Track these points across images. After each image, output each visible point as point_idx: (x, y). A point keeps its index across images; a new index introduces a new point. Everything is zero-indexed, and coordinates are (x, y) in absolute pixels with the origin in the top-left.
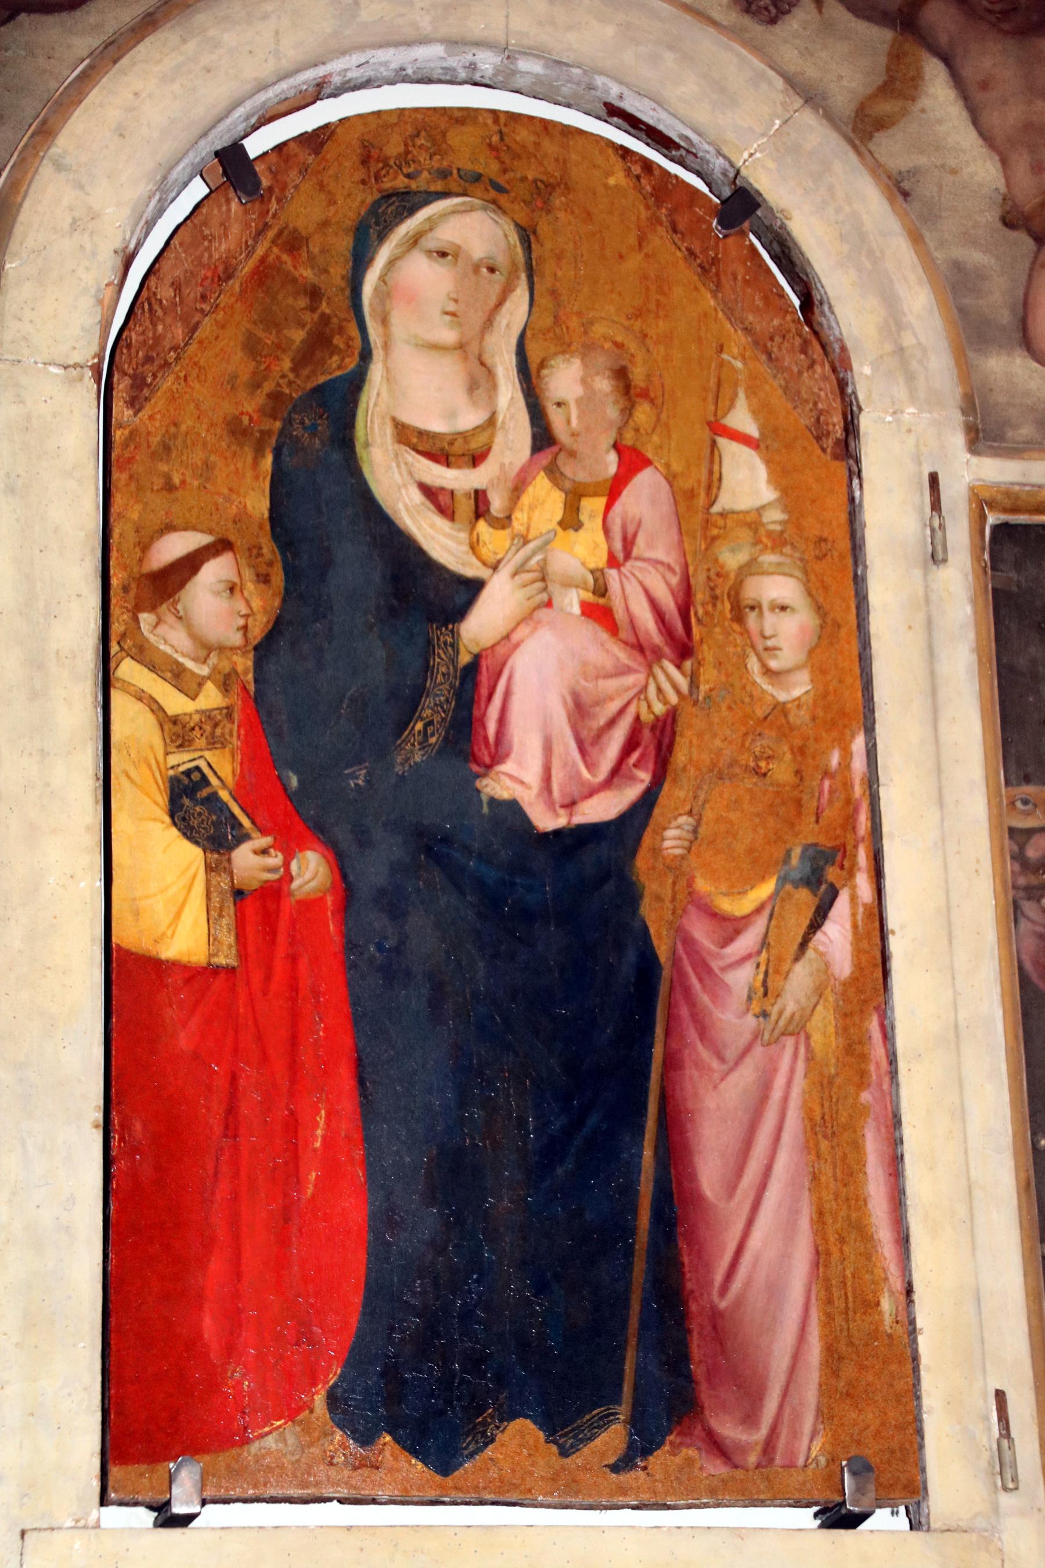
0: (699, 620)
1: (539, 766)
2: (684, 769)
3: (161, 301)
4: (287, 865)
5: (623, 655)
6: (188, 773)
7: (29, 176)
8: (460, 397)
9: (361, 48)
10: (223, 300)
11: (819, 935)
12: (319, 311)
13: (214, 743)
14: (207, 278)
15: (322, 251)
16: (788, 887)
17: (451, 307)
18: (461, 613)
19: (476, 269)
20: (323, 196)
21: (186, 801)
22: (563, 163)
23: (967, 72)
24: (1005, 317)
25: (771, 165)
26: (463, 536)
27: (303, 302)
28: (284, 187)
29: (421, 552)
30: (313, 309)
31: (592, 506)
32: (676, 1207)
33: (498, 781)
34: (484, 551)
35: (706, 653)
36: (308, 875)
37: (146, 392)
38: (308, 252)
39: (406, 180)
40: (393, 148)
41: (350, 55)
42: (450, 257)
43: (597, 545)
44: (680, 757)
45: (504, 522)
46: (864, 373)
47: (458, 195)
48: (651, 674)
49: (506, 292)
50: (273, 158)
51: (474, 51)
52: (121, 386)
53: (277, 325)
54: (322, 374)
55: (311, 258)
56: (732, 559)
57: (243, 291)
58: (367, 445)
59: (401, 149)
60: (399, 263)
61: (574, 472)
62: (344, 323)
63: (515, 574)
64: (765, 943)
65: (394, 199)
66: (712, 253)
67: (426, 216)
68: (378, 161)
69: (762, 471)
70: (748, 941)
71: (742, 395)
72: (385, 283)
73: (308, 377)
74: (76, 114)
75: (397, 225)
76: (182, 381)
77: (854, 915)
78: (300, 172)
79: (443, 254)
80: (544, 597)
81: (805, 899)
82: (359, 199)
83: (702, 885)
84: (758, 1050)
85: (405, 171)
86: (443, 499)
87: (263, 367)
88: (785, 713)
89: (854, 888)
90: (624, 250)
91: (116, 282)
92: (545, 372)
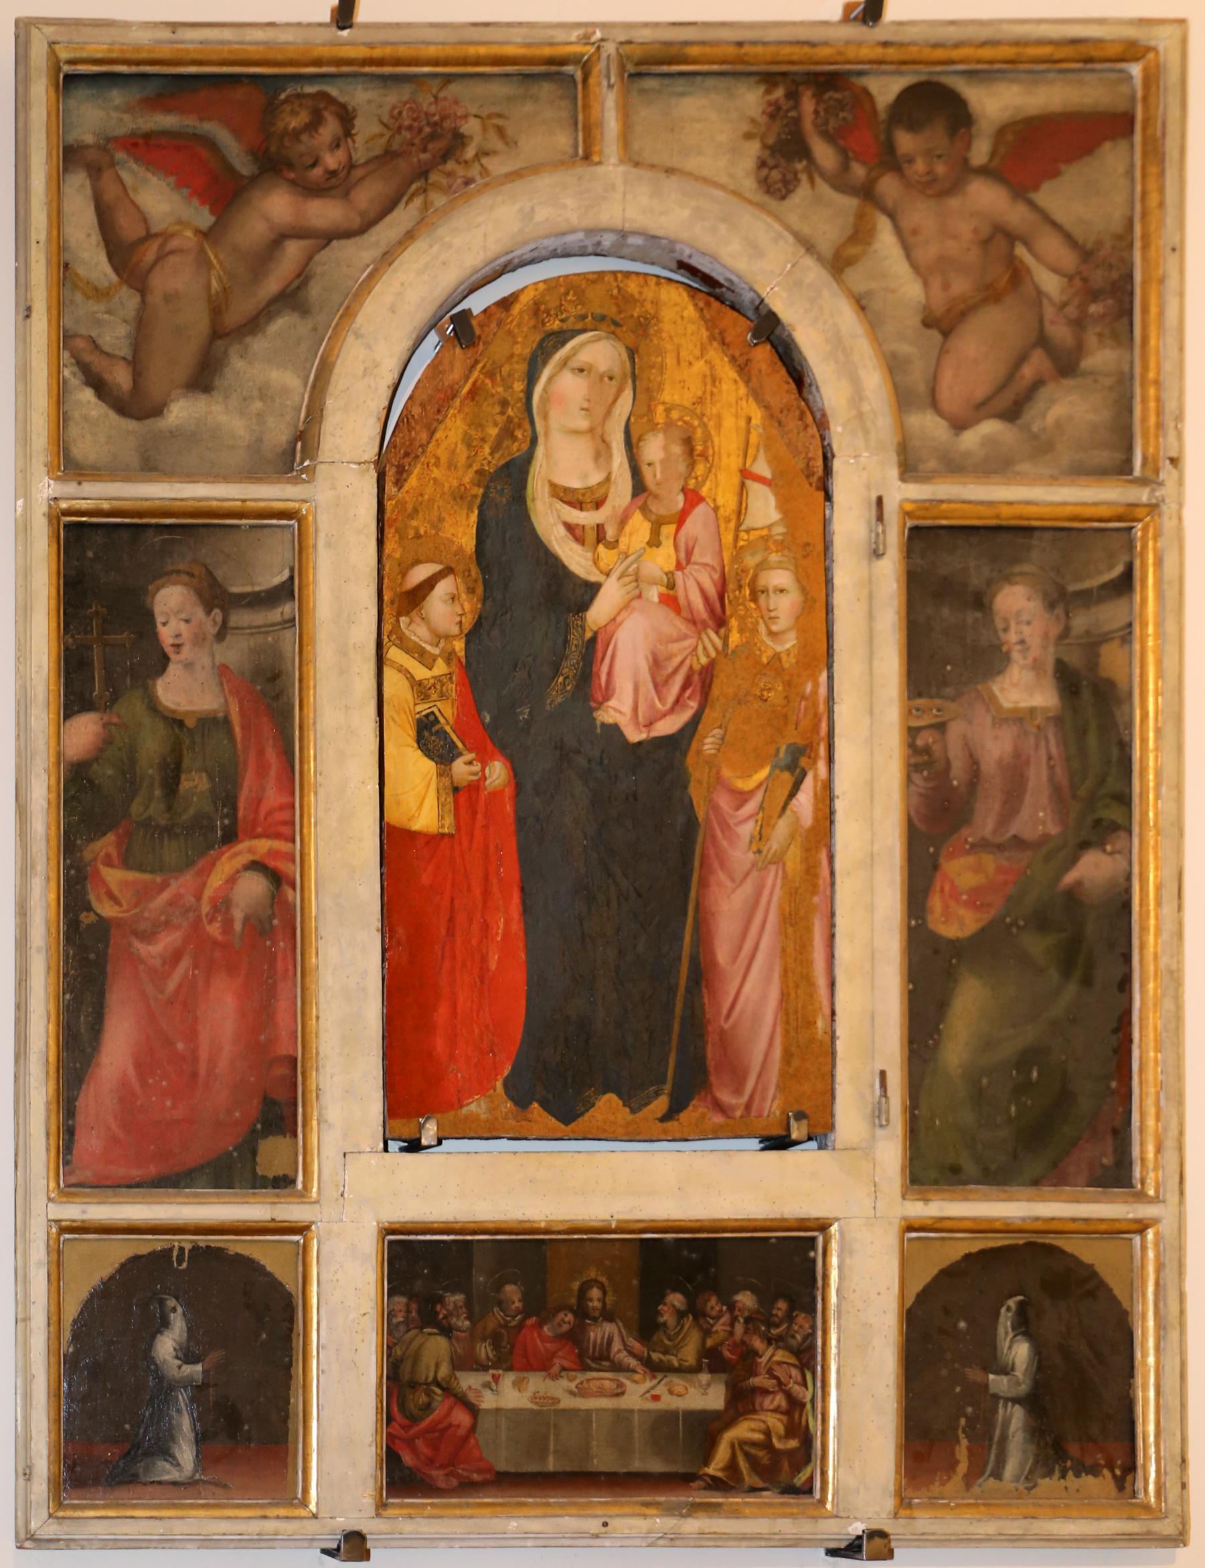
0: (730, 602)
1: (630, 704)
2: (718, 699)
4: (483, 770)
5: (683, 627)
6: (427, 716)
8: (589, 464)
10: (452, 411)
11: (794, 801)
13: (443, 696)
15: (509, 375)
16: (777, 771)
17: (585, 405)
18: (585, 606)
19: (601, 377)
21: (426, 734)
22: (656, 303)
23: (905, 224)
24: (922, 388)
25: (784, 295)
26: (589, 555)
27: (498, 409)
29: (564, 567)
30: (502, 413)
31: (668, 530)
32: (702, 974)
33: (607, 712)
34: (602, 564)
35: (734, 623)
36: (495, 777)
37: (405, 475)
43: (670, 556)
44: (716, 691)
45: (613, 545)
46: (838, 433)
48: (700, 638)
49: (620, 391)
56: (751, 561)
58: (533, 500)
59: (558, 303)
61: (657, 508)
63: (619, 578)
64: (761, 807)
66: (746, 357)
69: (772, 501)
70: (751, 807)
71: (762, 451)
77: (815, 787)
79: (581, 370)
80: (637, 591)
81: (787, 778)
83: (726, 773)
84: (754, 874)
86: (578, 532)
88: (780, 660)
89: (816, 770)
90: (691, 358)
92: (641, 444)
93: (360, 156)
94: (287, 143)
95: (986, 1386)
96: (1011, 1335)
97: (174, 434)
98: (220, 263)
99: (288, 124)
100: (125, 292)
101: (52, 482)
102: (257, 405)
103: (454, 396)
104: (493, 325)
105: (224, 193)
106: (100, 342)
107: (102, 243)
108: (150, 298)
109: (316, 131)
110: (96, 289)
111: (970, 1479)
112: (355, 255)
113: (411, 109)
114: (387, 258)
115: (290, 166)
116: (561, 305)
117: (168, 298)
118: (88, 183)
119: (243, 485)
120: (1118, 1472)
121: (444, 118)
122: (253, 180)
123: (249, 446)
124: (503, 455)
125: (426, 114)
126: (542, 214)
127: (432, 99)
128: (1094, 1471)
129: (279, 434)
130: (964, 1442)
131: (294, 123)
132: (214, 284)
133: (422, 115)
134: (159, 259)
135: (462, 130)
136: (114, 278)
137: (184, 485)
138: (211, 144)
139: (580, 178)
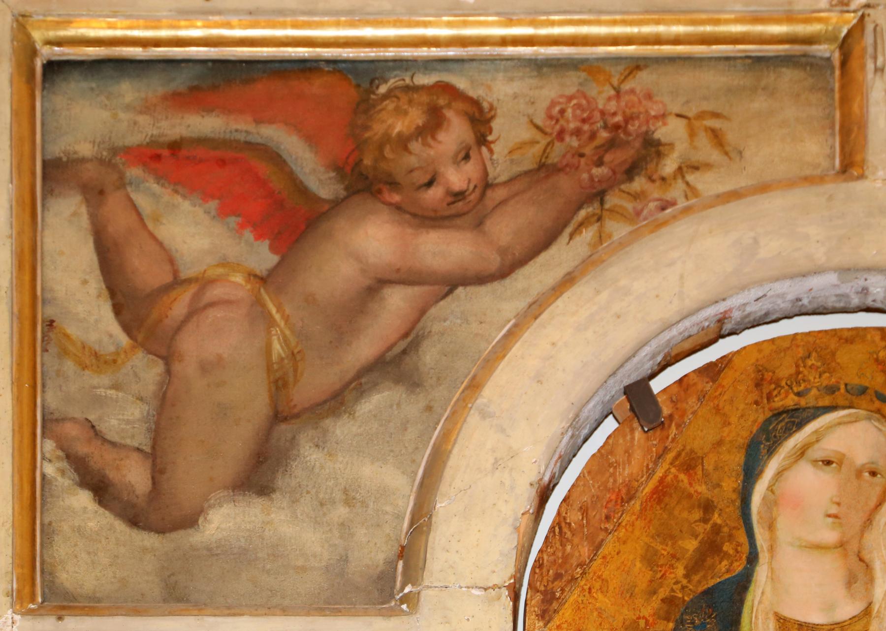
3: (570, 524)
7: (459, 426)
8: (838, 591)
9: (760, 283)
10: (626, 518)
12: (711, 522)
14: (611, 500)
15: (716, 469)
17: (834, 510)
19: (859, 473)
20: (718, 419)
27: (697, 515)
28: (683, 414)
30: (705, 521)
37: (555, 605)
38: (703, 470)
39: (796, 398)
40: (785, 371)
41: (749, 290)
42: (834, 465)
47: (844, 408)
50: (676, 389)
51: (865, 276)
52: (533, 602)
53: (672, 537)
54: (712, 578)
55: (706, 475)
57: (643, 509)
59: (793, 370)
60: (786, 473)
62: (734, 531)
65: (784, 415)
67: (813, 430)
68: (770, 383)
72: (772, 491)
73: (699, 582)
74: (500, 367)
75: (786, 439)
76: (587, 593)
78: (699, 399)
79: (828, 463)
82: (751, 419)
85: (795, 389)
87: (659, 575)
91: (531, 511)
93: (500, 171)
94: (388, 152)
97: (211, 552)
98: (287, 319)
99: (392, 127)
100: (140, 359)
101: (17, 617)
102: (341, 512)
103: (631, 498)
104: (692, 401)
105: (291, 222)
106: (102, 427)
107: (105, 293)
108: (177, 367)
109: (434, 138)
110: (96, 355)
112: (490, 307)
113: (578, 106)
114: (536, 309)
115: (394, 185)
116: (798, 373)
117: (205, 368)
118: (84, 210)
119: (310, 619)
121: (628, 119)
122: (336, 204)
123: (327, 567)
124: (705, 577)
125: (603, 113)
126: (772, 247)
127: (612, 92)
129: (373, 550)
131: (400, 126)
132: (277, 348)
133: (597, 115)
134: (193, 312)
135: (657, 135)
136: (123, 339)
137: (220, 619)
138: (275, 158)
139: (830, 198)
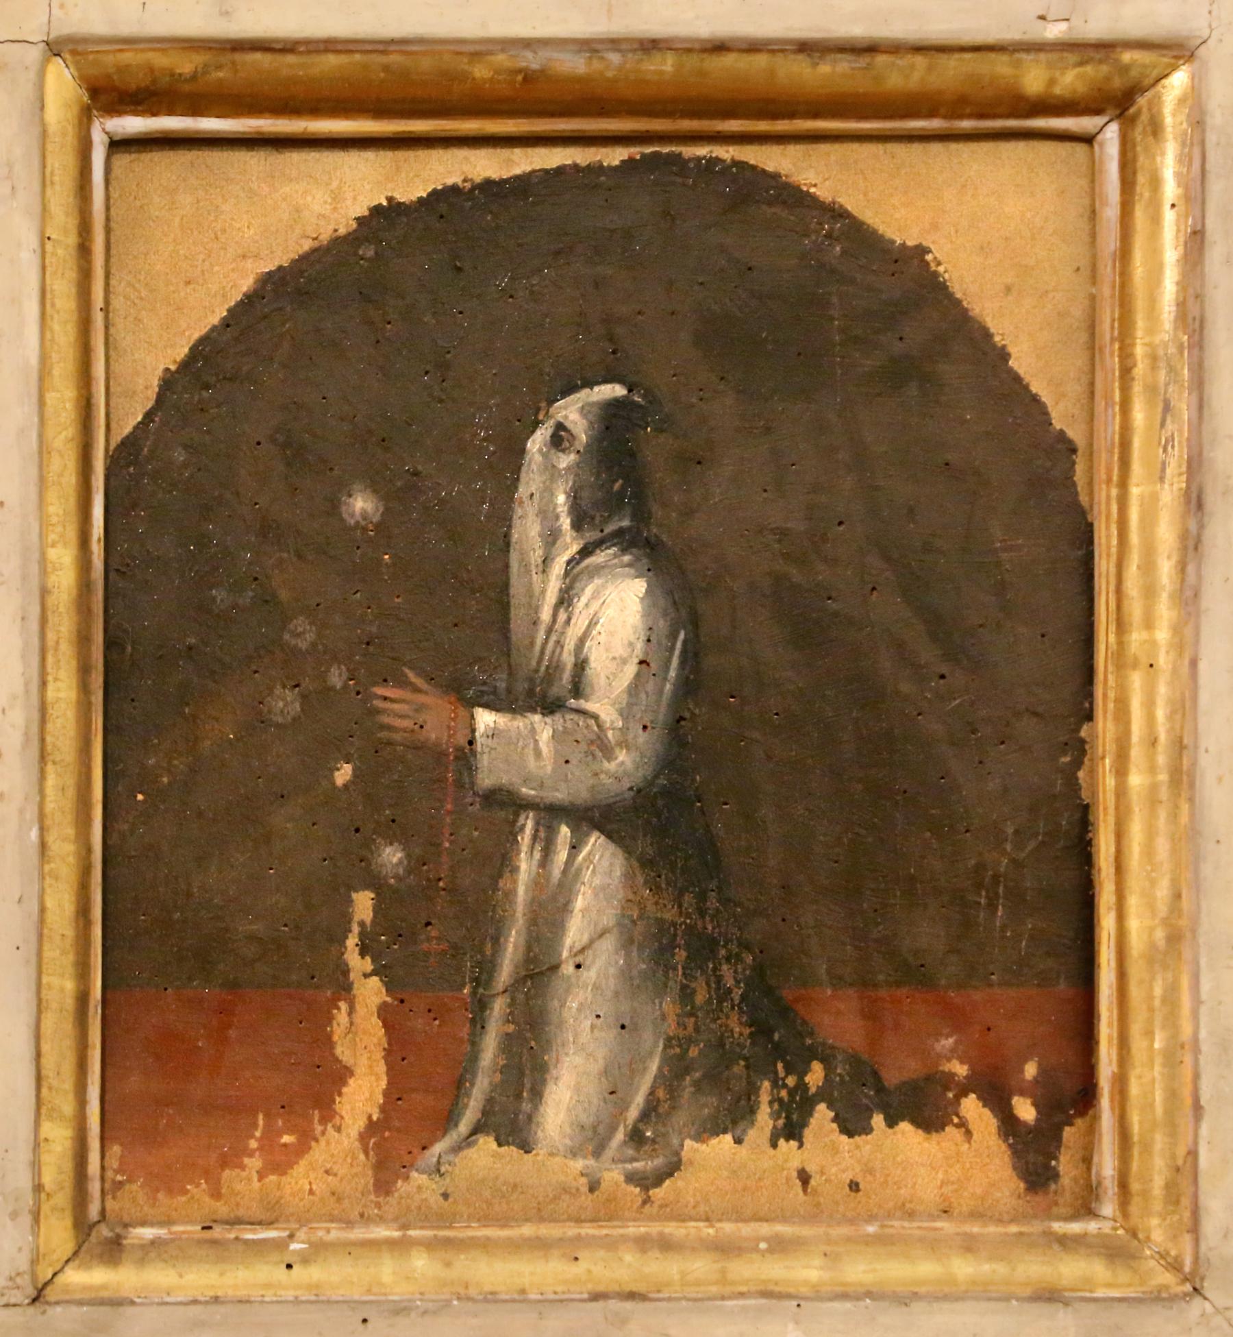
95: (466, 754)
96: (570, 545)
111: (396, 1142)
120: (1025, 1111)
128: (925, 1106)
130: (370, 992)
